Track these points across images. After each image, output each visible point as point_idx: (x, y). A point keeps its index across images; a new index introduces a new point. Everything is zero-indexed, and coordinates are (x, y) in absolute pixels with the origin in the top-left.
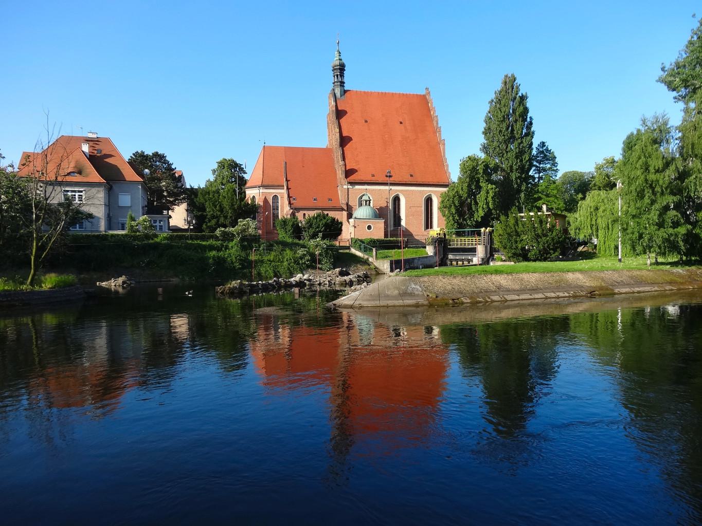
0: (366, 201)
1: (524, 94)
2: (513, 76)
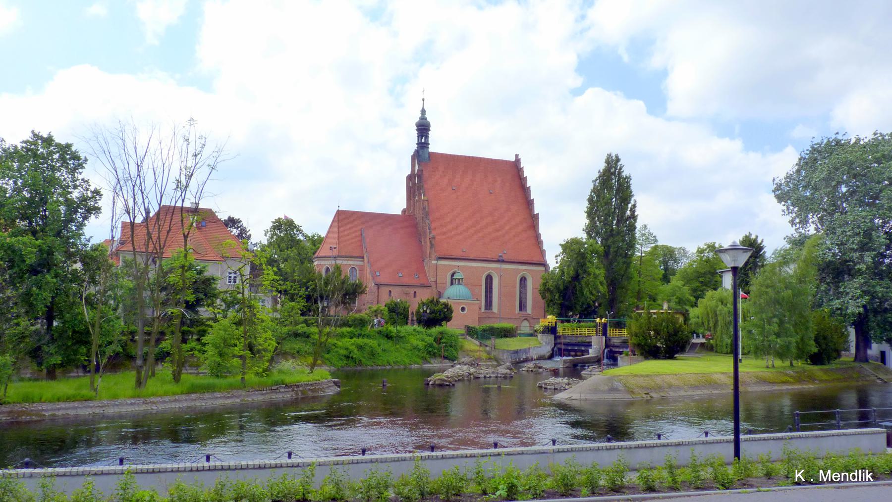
0: (459, 280)
1: (628, 175)
2: (617, 157)
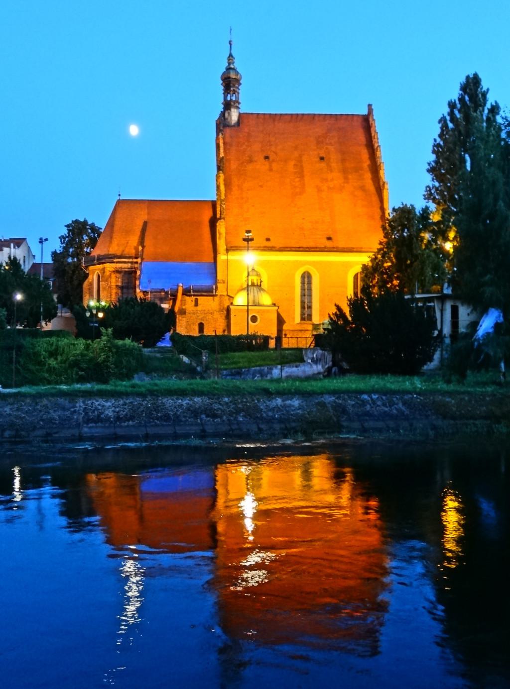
1: (494, 104)
